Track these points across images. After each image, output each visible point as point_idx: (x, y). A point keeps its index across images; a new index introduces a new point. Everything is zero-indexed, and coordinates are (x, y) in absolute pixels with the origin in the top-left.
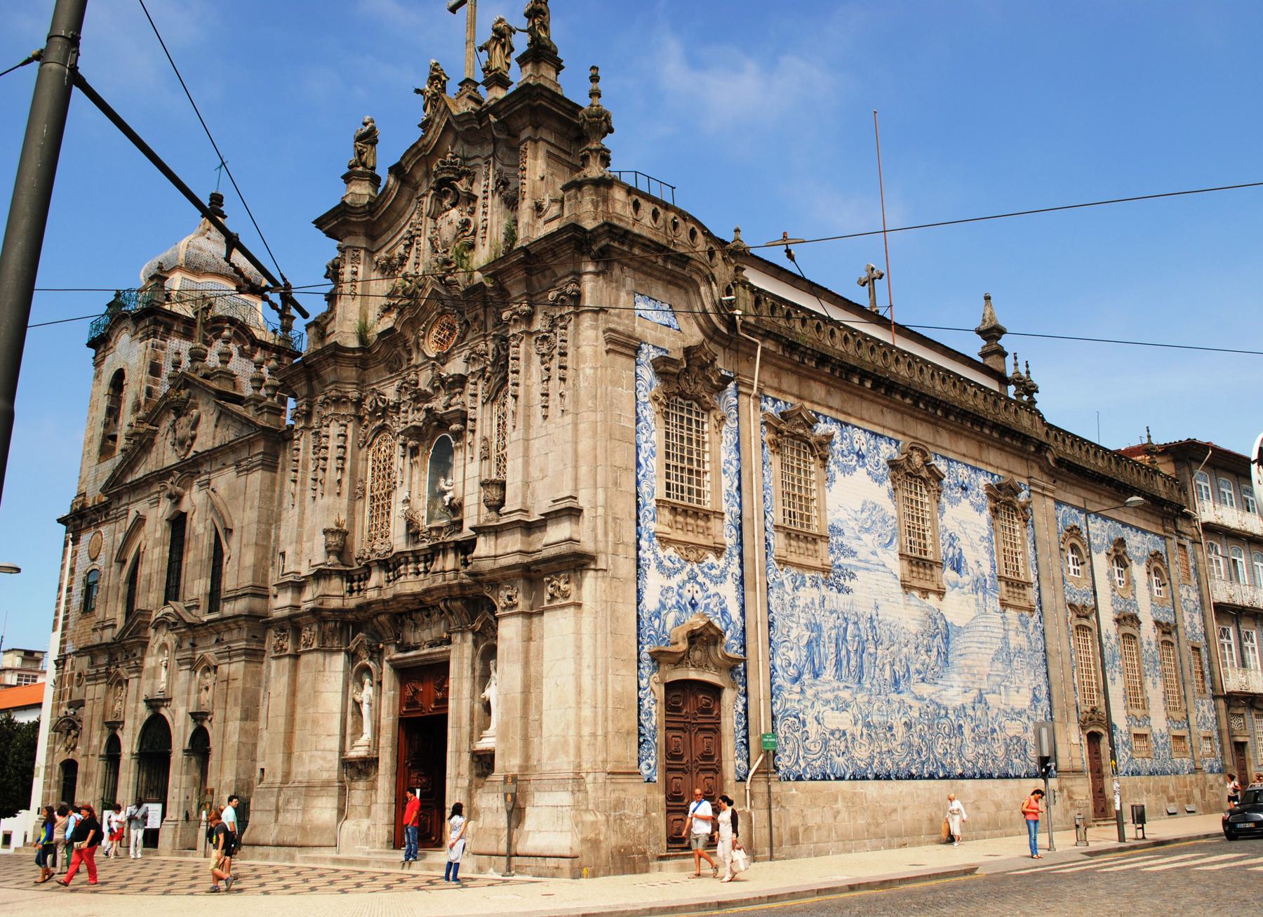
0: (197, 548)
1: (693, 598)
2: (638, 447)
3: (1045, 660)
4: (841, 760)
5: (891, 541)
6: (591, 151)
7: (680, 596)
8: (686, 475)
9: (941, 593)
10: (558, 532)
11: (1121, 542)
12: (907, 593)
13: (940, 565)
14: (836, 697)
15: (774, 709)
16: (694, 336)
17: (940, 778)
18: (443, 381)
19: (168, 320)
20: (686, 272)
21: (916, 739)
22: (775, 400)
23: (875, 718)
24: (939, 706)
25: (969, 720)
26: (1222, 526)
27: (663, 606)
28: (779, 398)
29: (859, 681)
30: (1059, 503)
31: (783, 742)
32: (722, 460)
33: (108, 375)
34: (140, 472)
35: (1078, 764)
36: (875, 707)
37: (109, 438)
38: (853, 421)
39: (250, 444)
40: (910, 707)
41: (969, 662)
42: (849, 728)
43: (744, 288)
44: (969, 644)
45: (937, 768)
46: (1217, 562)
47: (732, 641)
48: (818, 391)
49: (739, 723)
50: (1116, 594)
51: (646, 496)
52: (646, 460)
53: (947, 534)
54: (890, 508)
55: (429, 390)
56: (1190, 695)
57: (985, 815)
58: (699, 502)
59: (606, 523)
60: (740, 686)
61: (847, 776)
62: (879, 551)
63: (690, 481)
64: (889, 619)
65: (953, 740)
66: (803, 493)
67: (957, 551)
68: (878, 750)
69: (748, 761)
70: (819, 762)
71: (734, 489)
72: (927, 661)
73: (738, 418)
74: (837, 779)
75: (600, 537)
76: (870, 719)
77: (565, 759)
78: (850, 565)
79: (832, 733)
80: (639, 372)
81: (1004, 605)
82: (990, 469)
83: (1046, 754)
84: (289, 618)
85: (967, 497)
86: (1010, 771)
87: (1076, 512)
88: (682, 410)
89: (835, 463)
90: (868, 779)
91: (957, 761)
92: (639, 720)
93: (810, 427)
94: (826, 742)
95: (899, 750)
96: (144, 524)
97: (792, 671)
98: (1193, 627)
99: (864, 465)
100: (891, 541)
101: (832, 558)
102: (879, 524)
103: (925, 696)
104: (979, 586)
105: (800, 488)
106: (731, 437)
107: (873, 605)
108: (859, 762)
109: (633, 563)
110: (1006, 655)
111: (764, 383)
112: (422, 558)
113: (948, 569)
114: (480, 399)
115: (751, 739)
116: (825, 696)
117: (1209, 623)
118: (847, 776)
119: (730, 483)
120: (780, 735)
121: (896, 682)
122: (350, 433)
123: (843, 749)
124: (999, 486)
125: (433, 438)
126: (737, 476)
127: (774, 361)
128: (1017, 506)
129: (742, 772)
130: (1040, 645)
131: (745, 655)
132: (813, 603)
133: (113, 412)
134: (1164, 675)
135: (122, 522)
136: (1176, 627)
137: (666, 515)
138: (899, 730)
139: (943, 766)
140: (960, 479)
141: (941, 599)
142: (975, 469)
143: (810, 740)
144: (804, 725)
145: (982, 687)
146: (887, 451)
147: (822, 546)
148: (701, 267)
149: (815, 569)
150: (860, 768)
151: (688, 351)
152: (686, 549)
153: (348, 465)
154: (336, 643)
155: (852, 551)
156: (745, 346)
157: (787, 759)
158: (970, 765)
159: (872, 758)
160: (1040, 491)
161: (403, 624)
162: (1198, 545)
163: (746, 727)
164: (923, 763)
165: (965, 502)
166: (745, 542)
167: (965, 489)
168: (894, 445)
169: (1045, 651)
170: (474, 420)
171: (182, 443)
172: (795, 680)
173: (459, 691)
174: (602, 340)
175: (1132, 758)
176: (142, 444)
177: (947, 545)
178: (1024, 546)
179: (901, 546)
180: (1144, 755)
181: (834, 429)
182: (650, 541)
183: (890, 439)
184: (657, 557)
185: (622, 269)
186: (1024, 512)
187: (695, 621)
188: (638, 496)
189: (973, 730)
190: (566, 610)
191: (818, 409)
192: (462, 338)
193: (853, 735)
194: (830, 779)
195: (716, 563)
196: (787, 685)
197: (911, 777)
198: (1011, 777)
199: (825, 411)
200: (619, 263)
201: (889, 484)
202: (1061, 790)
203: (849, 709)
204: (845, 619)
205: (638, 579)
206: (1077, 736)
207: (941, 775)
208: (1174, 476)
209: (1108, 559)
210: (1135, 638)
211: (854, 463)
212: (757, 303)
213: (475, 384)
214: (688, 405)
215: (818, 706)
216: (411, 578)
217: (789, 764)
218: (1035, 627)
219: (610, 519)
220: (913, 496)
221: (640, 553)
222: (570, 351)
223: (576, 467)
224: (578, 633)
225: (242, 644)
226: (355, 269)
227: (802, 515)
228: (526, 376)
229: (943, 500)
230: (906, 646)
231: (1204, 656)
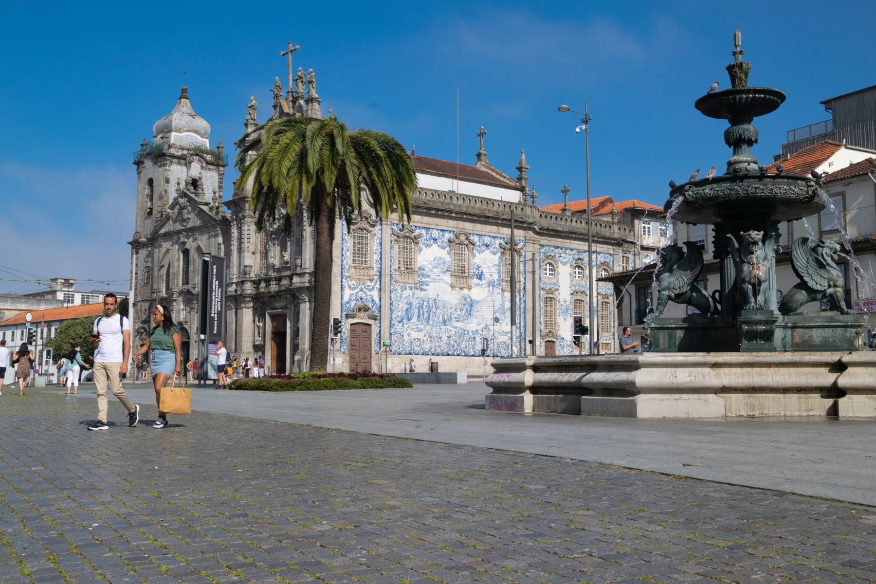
2: (342, 249)
4: (418, 348)
7: (356, 296)
8: (360, 256)
9: (470, 288)
14: (417, 327)
24: (465, 330)
27: (350, 300)
30: (542, 246)
33: (145, 180)
38: (432, 226)
41: (482, 314)
50: (574, 282)
54: (448, 258)
62: (441, 275)
66: (408, 257)
67: (480, 271)
69: (380, 348)
79: (415, 339)
81: (503, 290)
83: (485, 349)
86: (499, 355)
87: (553, 249)
88: (360, 233)
91: (472, 350)
94: (411, 342)
97: (399, 319)
99: (437, 243)
101: (419, 279)
104: (491, 284)
105: (407, 255)
106: (378, 241)
113: (475, 279)
121: (445, 322)
123: (419, 344)
132: (409, 295)
137: (353, 270)
138: (445, 339)
139: (464, 351)
140: (485, 242)
142: (494, 237)
144: (403, 336)
146: (447, 236)
149: (411, 283)
158: (478, 352)
164: (455, 350)
165: (487, 252)
167: (487, 246)
170: (293, 232)
181: (424, 232)
182: (346, 279)
184: (348, 284)
187: (360, 303)
191: (416, 224)
195: (370, 284)
196: (397, 324)
201: (448, 249)
204: (423, 300)
211: (432, 243)
215: (409, 330)
220: (460, 252)
229: (475, 251)
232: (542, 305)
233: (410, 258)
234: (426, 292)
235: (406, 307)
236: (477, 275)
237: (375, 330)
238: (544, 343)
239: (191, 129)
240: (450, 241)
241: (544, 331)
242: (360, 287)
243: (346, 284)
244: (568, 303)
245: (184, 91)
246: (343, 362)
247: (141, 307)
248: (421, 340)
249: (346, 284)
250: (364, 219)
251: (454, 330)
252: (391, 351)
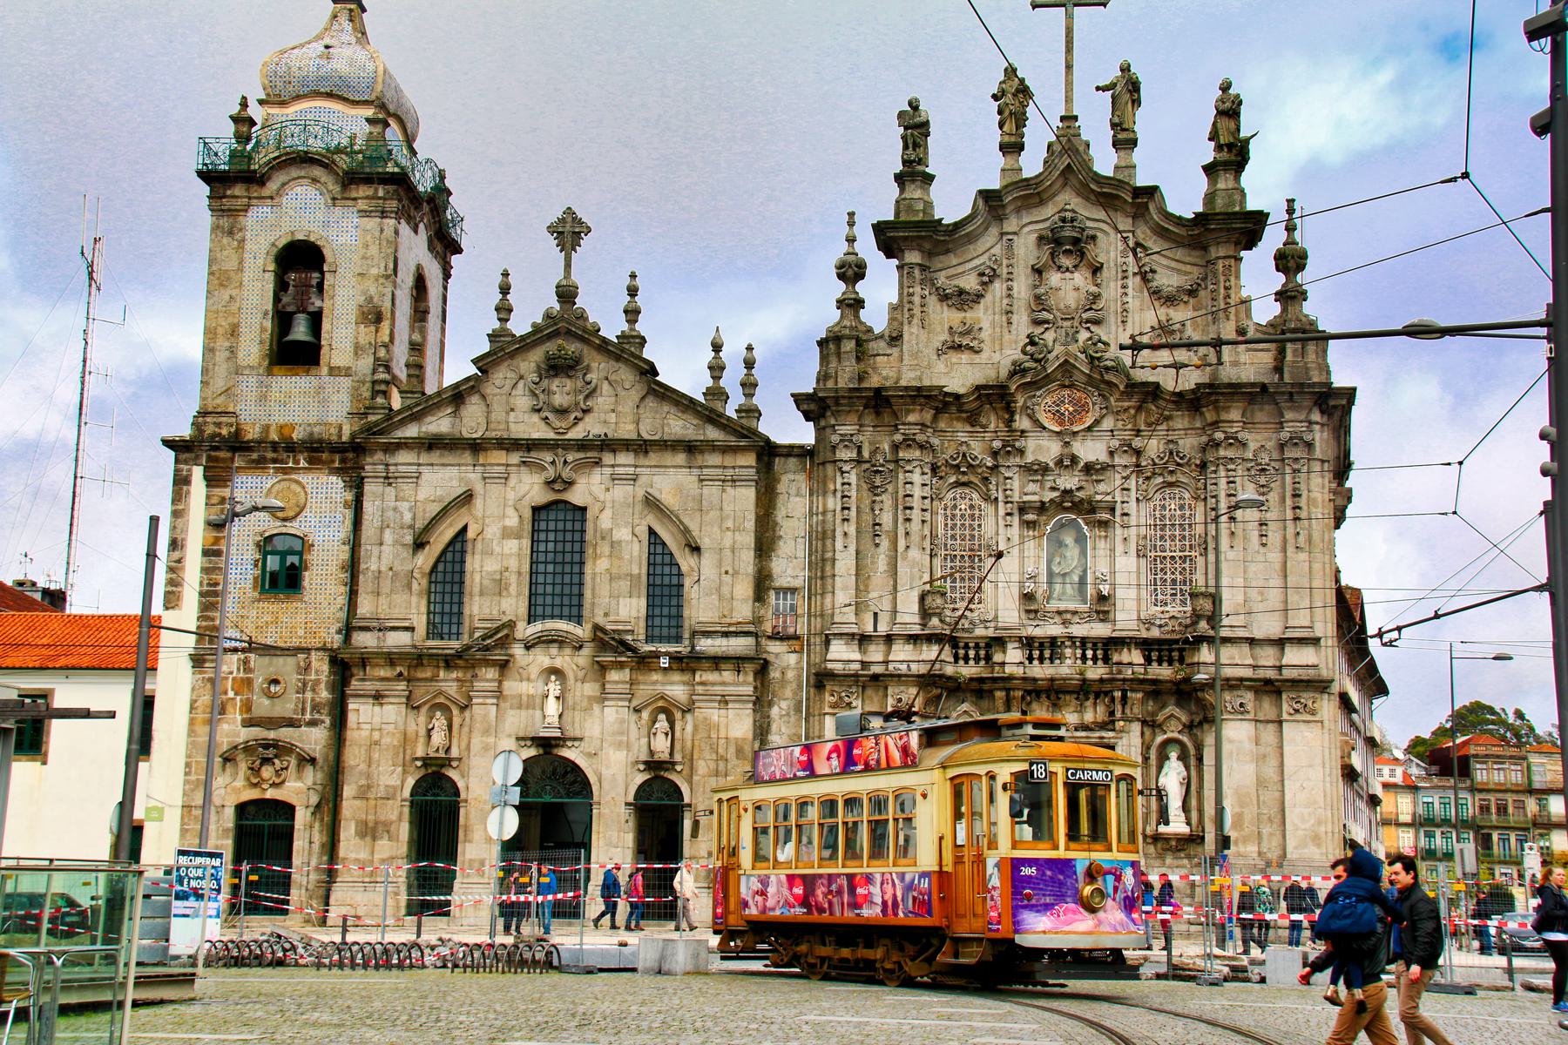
18: (1074, 459)
34: (439, 424)
55: (1052, 465)
75: (1331, 665)
77: (1316, 850)
112: (1090, 645)
114: (1133, 494)
135: (407, 488)
161: (1029, 704)
171: (562, 412)
174: (1326, 490)
190: (1312, 725)
192: (1097, 422)
216: (1079, 662)
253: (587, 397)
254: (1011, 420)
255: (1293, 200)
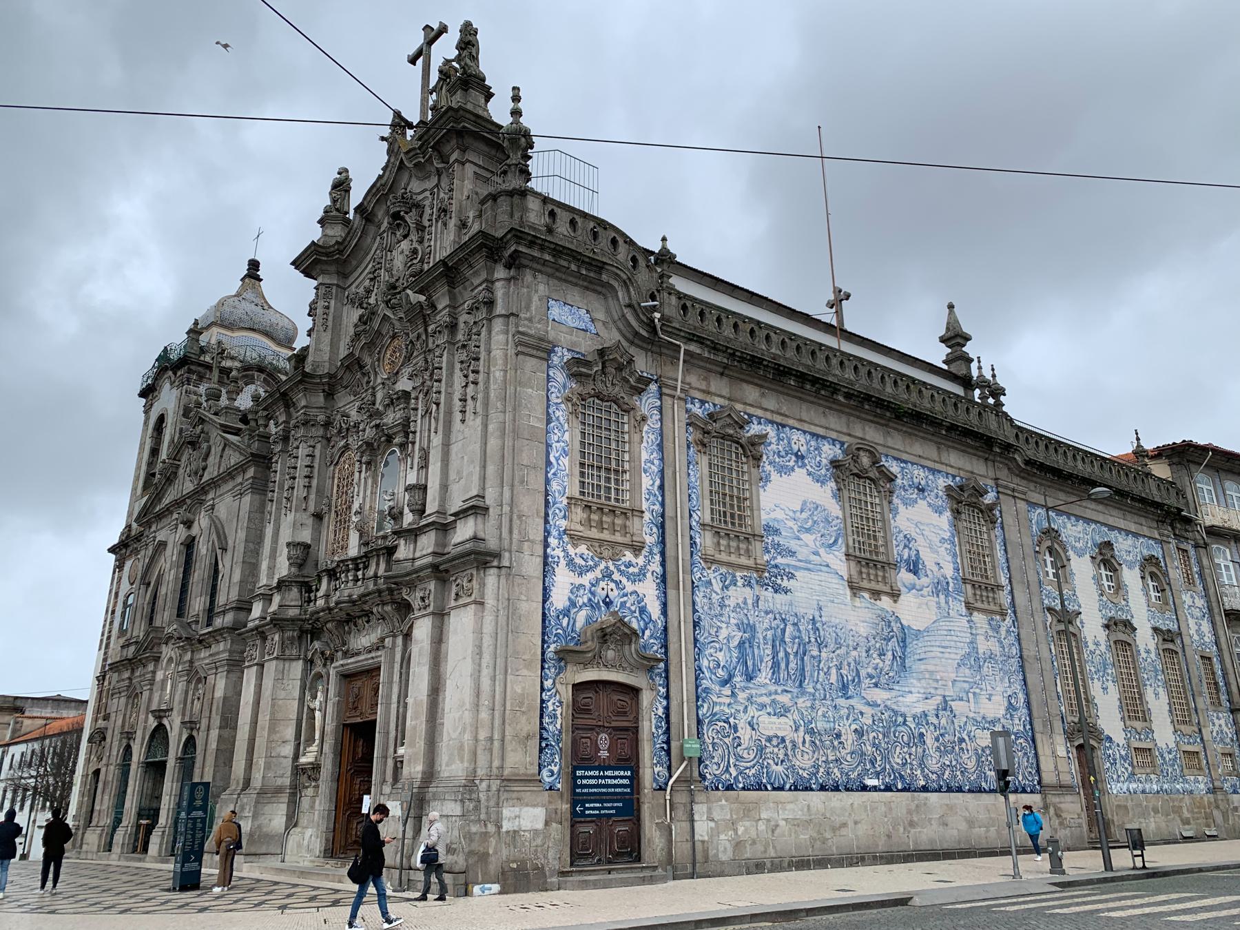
0: (200, 568)
1: (607, 596)
2: (548, 446)
3: (1022, 667)
4: (780, 768)
5: (836, 541)
6: (509, 166)
7: (593, 594)
8: (603, 474)
9: (895, 595)
10: (464, 531)
11: (1109, 544)
12: (854, 595)
13: (895, 566)
14: (773, 701)
15: (700, 712)
16: (611, 337)
17: (898, 791)
19: (200, 369)
20: (604, 277)
21: (869, 748)
22: (703, 402)
23: (820, 725)
24: (896, 713)
25: (932, 728)
26: (1229, 529)
28: (708, 399)
29: (801, 686)
30: (1034, 505)
31: (711, 749)
32: (643, 460)
34: (166, 500)
35: (1066, 779)
36: (820, 713)
37: (150, 475)
38: (791, 422)
39: (241, 468)
40: (862, 713)
41: (931, 668)
42: (789, 734)
43: (670, 294)
44: (932, 649)
45: (895, 778)
46: (1227, 567)
47: (652, 641)
48: (751, 393)
49: (657, 727)
50: (1105, 599)
51: (557, 494)
52: (557, 459)
53: (902, 535)
54: (835, 509)
56: (1201, 705)
57: (955, 832)
58: (617, 500)
59: (511, 520)
60: (661, 688)
61: (788, 786)
62: (822, 551)
63: (608, 480)
64: (835, 621)
65: (914, 749)
67: (913, 553)
68: (824, 759)
69: (669, 768)
70: (753, 771)
71: (656, 488)
72: (881, 665)
73: (661, 420)
74: (774, 789)
75: (505, 534)
76: (813, 725)
78: (788, 565)
79: (769, 739)
80: (551, 373)
81: (970, 608)
82: (950, 470)
83: (1005, 767)
84: (256, 628)
85: (924, 498)
86: (983, 784)
89: (770, 463)
90: (812, 790)
91: (919, 772)
92: (541, 723)
93: (742, 427)
94: (761, 750)
95: (849, 758)
96: (165, 549)
97: (720, 672)
98: (1201, 636)
99: (804, 466)
100: (836, 541)
101: (766, 557)
102: (822, 525)
103: (879, 702)
104: (940, 587)
105: (731, 487)
106: (652, 437)
107: (816, 607)
108: (801, 772)
109: (539, 561)
110: (974, 660)
111: (689, 384)
112: (361, 566)
113: (903, 570)
115: (674, 744)
116: (760, 700)
117: (1221, 633)
118: (788, 786)
119: (651, 482)
120: (707, 740)
121: (844, 687)
122: (317, 453)
123: (781, 757)
124: (961, 488)
125: (384, 453)
126: (659, 474)
127: (702, 364)
128: (983, 507)
129: (662, 780)
130: (1014, 651)
131: (666, 653)
132: (745, 603)
133: (155, 452)
134: (1167, 684)
136: (1180, 634)
137: (579, 514)
138: (849, 738)
139: (902, 777)
140: (916, 481)
141: (895, 601)
143: (743, 747)
144: (736, 730)
145: (947, 693)
146: (830, 451)
147: (757, 547)
148: (619, 272)
149: (748, 568)
150: (802, 777)
151: (602, 353)
152: (600, 546)
153: (315, 482)
154: (294, 652)
155: (790, 551)
156: (668, 349)
157: (715, 767)
158: (934, 777)
159: (816, 767)
160: (1010, 492)
161: (349, 633)
162: (1202, 551)
163: (668, 729)
165: (922, 504)
166: (667, 540)
167: (922, 490)
168: (838, 446)
169: (1021, 657)
170: (414, 433)
171: (196, 473)
172: (725, 682)
173: (389, 696)
175: (1133, 774)
176: (170, 477)
177: (901, 547)
178: (992, 548)
179: (847, 546)
180: (1148, 770)
181: (771, 431)
182: (560, 538)
183: (834, 440)
184: (567, 555)
185: (535, 277)
186: (988, 514)
188: (547, 495)
189: (937, 739)
190: (468, 608)
191: (751, 410)
192: (408, 358)
193: (793, 742)
194: (766, 789)
195: (634, 561)
196: (717, 688)
197: (864, 788)
198: (985, 791)
199: (759, 412)
200: (531, 268)
201: (833, 485)
202: (1046, 807)
203: (788, 714)
204: (783, 620)
205: (545, 576)
206: (1064, 749)
207: (900, 787)
208: (1170, 479)
209: (1093, 562)
210: (1129, 645)
211: (792, 463)
212: (684, 308)
213: (417, 398)
214: (606, 406)
215: (752, 711)
216: (350, 584)
217: (717, 772)
218: (1008, 631)
219: (515, 517)
220: (863, 498)
221: (549, 550)
222: (483, 356)
223: (484, 467)
224: (479, 632)
225: (225, 655)
226: (326, 304)
227: (732, 516)
228: (446, 384)
229: (896, 500)
230: (855, 649)
231: (1217, 667)
232: (1053, 651)
233: (739, 498)
234: (789, 596)
235: (738, 636)
236: (908, 562)
237: (651, 706)
238: (1074, 751)
239: (256, 327)
240: (835, 464)
241: (1070, 719)
242: (603, 565)
243: (559, 552)
244: (1103, 648)
245: (254, 265)
246: (547, 823)
247: (110, 683)
248: (787, 742)
249: (559, 552)
250: (611, 370)
251: (868, 711)
252: (703, 777)
253: (205, 459)
254: (368, 382)
255: (515, 89)
